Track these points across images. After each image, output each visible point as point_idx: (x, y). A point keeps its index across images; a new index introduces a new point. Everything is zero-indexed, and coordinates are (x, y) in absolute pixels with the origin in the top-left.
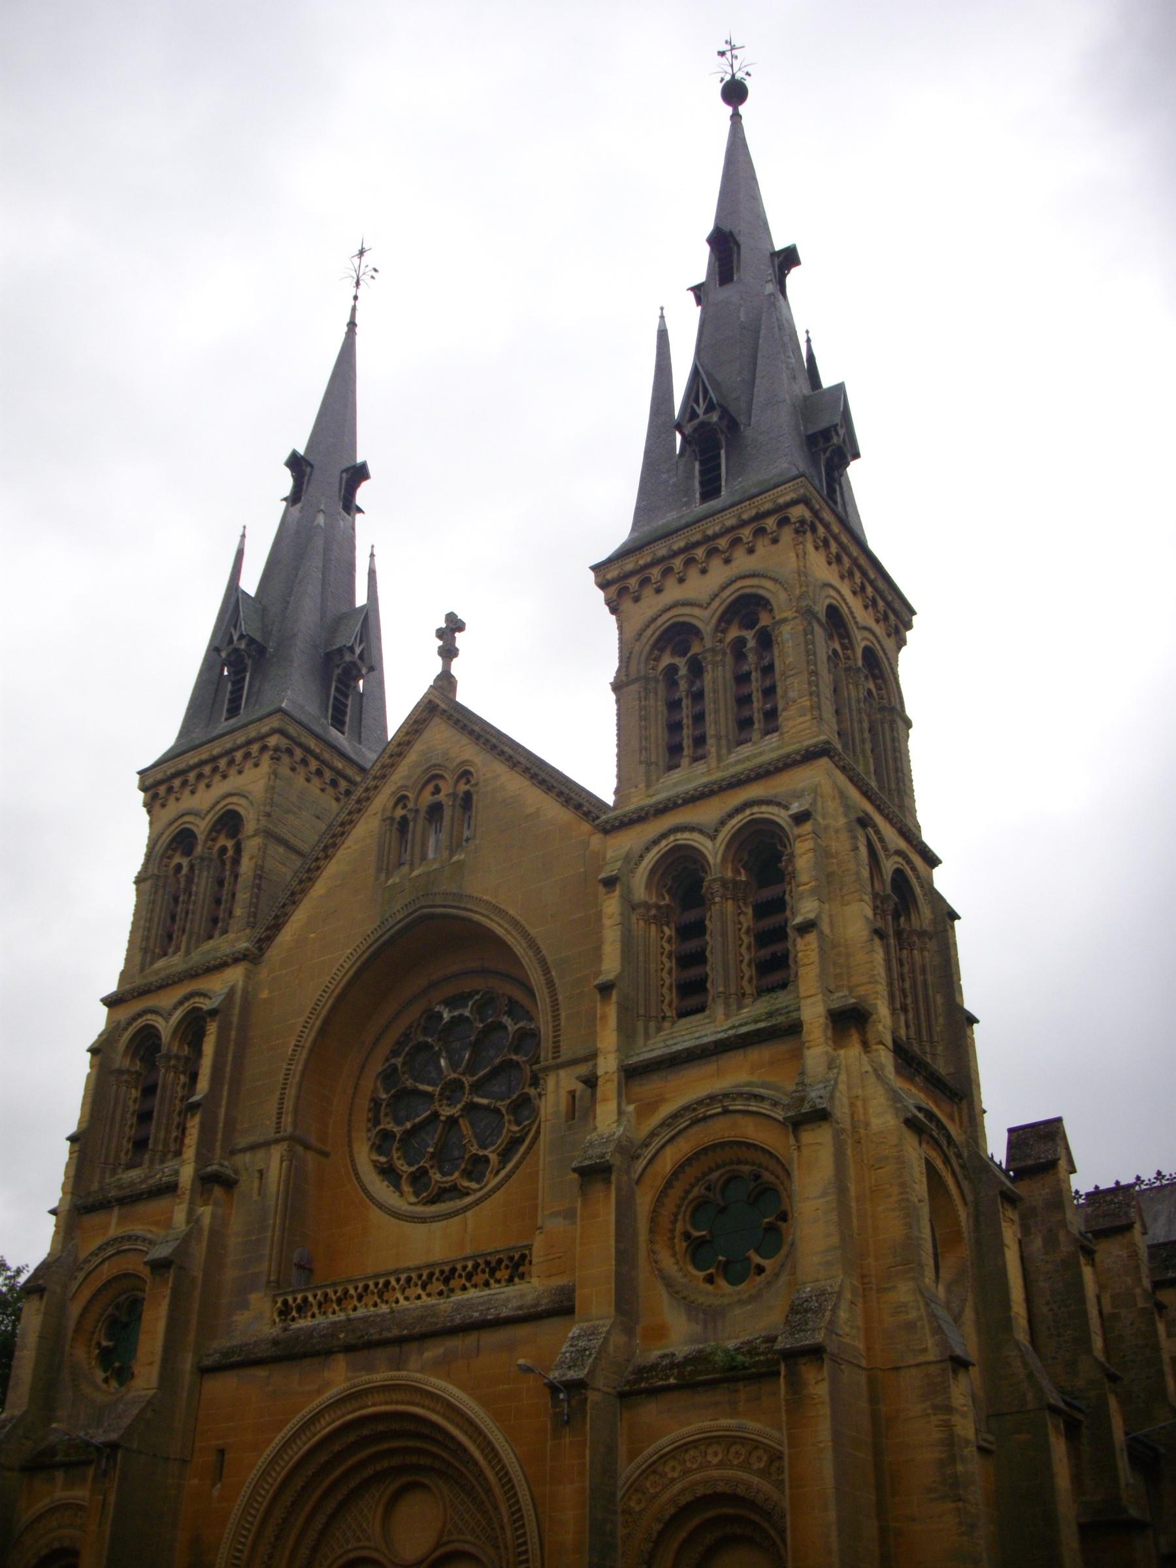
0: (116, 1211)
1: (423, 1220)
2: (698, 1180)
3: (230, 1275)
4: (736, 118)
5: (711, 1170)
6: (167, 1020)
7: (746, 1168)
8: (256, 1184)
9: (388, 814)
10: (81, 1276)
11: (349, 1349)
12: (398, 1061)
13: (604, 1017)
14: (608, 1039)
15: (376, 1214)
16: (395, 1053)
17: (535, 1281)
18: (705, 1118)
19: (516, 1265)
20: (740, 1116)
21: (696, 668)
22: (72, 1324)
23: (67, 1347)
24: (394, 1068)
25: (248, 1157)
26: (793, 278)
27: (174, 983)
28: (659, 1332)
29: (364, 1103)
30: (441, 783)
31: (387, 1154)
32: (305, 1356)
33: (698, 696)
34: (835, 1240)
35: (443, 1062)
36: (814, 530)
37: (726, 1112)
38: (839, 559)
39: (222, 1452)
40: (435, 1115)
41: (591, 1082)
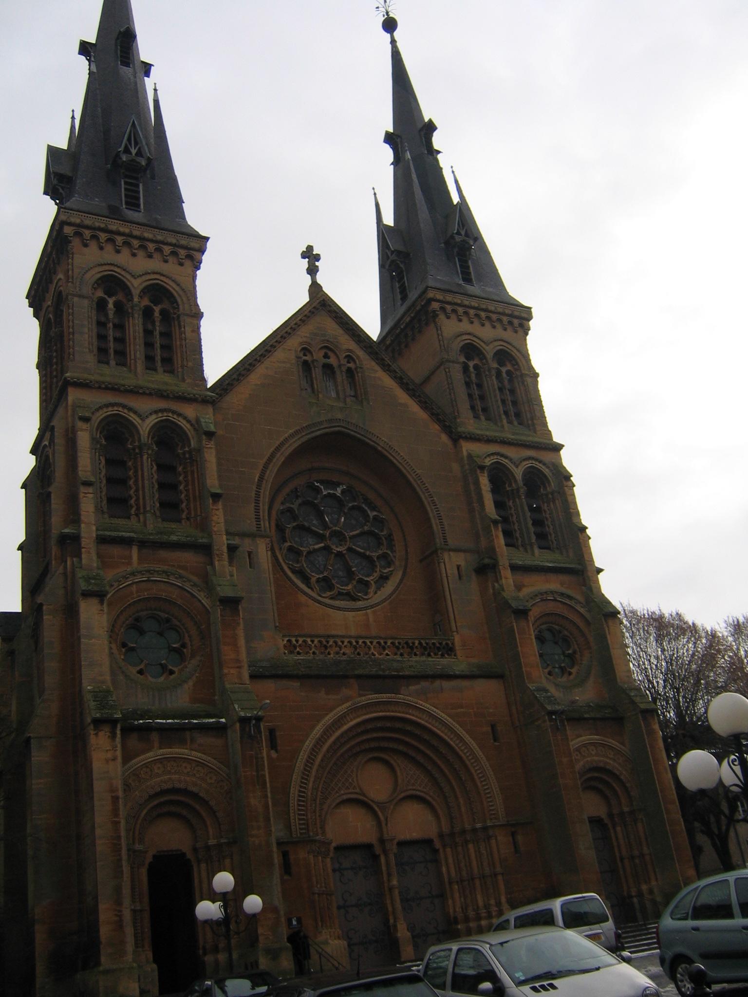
4: (393, 42)
5: (543, 624)
6: (143, 420)
13: (497, 536)
15: (303, 599)
24: (290, 510)
27: (144, 394)
30: (330, 353)
37: (555, 600)
40: (327, 548)
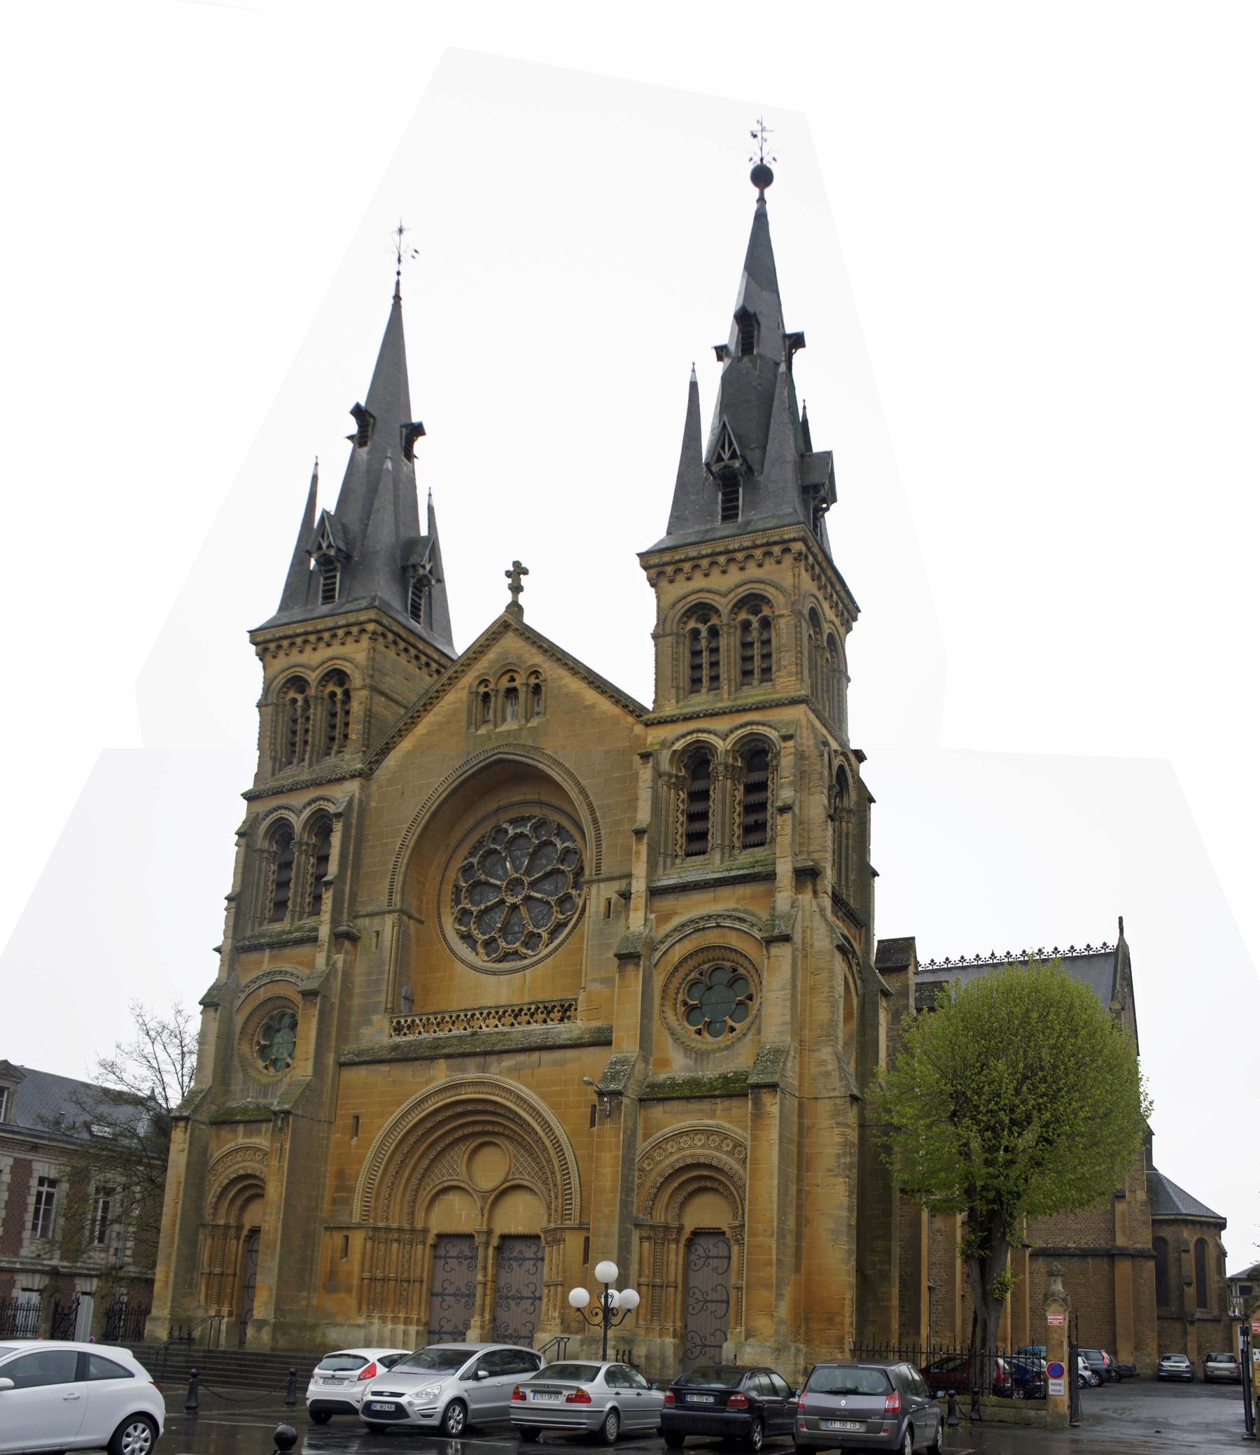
0: (268, 951)
1: (494, 973)
2: (695, 968)
3: (357, 1001)
5: (704, 963)
7: (729, 964)
8: (374, 941)
9: (474, 689)
10: (243, 996)
11: (448, 1056)
12: (475, 860)
14: (640, 869)
15: (459, 967)
16: (471, 854)
17: (579, 1023)
18: (703, 929)
19: (566, 1010)
20: (727, 930)
21: (714, 633)
22: (238, 1028)
23: (236, 1043)
24: (471, 865)
25: (367, 921)
26: (799, 357)
28: (665, 1063)
29: (448, 889)
31: (467, 925)
32: (416, 1059)
33: (715, 651)
34: (788, 1018)
35: (508, 865)
36: (806, 558)
37: (718, 926)
38: (819, 577)
39: (357, 1118)
40: (502, 902)
41: (626, 895)
